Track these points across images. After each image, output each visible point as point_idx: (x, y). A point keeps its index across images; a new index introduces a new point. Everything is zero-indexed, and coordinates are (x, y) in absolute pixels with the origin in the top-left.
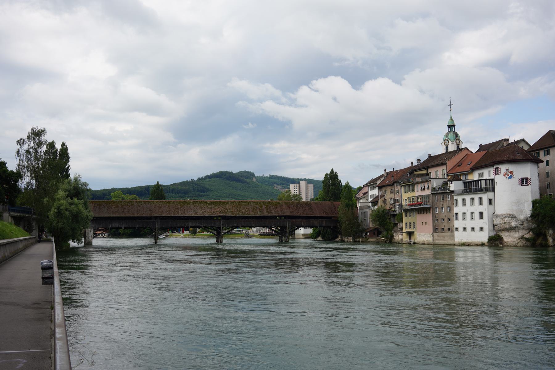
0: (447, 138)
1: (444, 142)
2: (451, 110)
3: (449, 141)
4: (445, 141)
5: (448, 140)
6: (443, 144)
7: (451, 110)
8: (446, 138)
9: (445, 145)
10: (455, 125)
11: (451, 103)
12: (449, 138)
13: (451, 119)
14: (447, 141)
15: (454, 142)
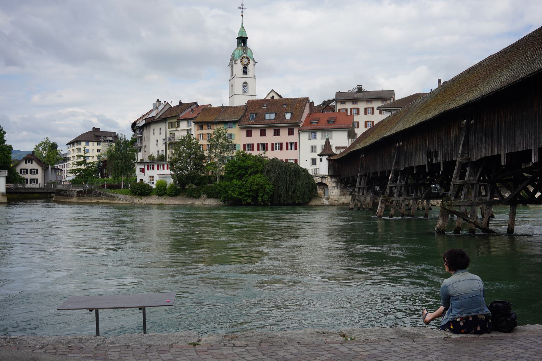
0: (245, 55)
1: (241, 60)
2: (242, 16)
3: (249, 60)
4: (242, 58)
5: (248, 58)
6: (239, 62)
7: (242, 16)
8: (242, 55)
9: (242, 64)
10: (247, 38)
11: (242, 5)
12: (249, 55)
13: (243, 27)
14: (245, 60)
15: (237, 62)
